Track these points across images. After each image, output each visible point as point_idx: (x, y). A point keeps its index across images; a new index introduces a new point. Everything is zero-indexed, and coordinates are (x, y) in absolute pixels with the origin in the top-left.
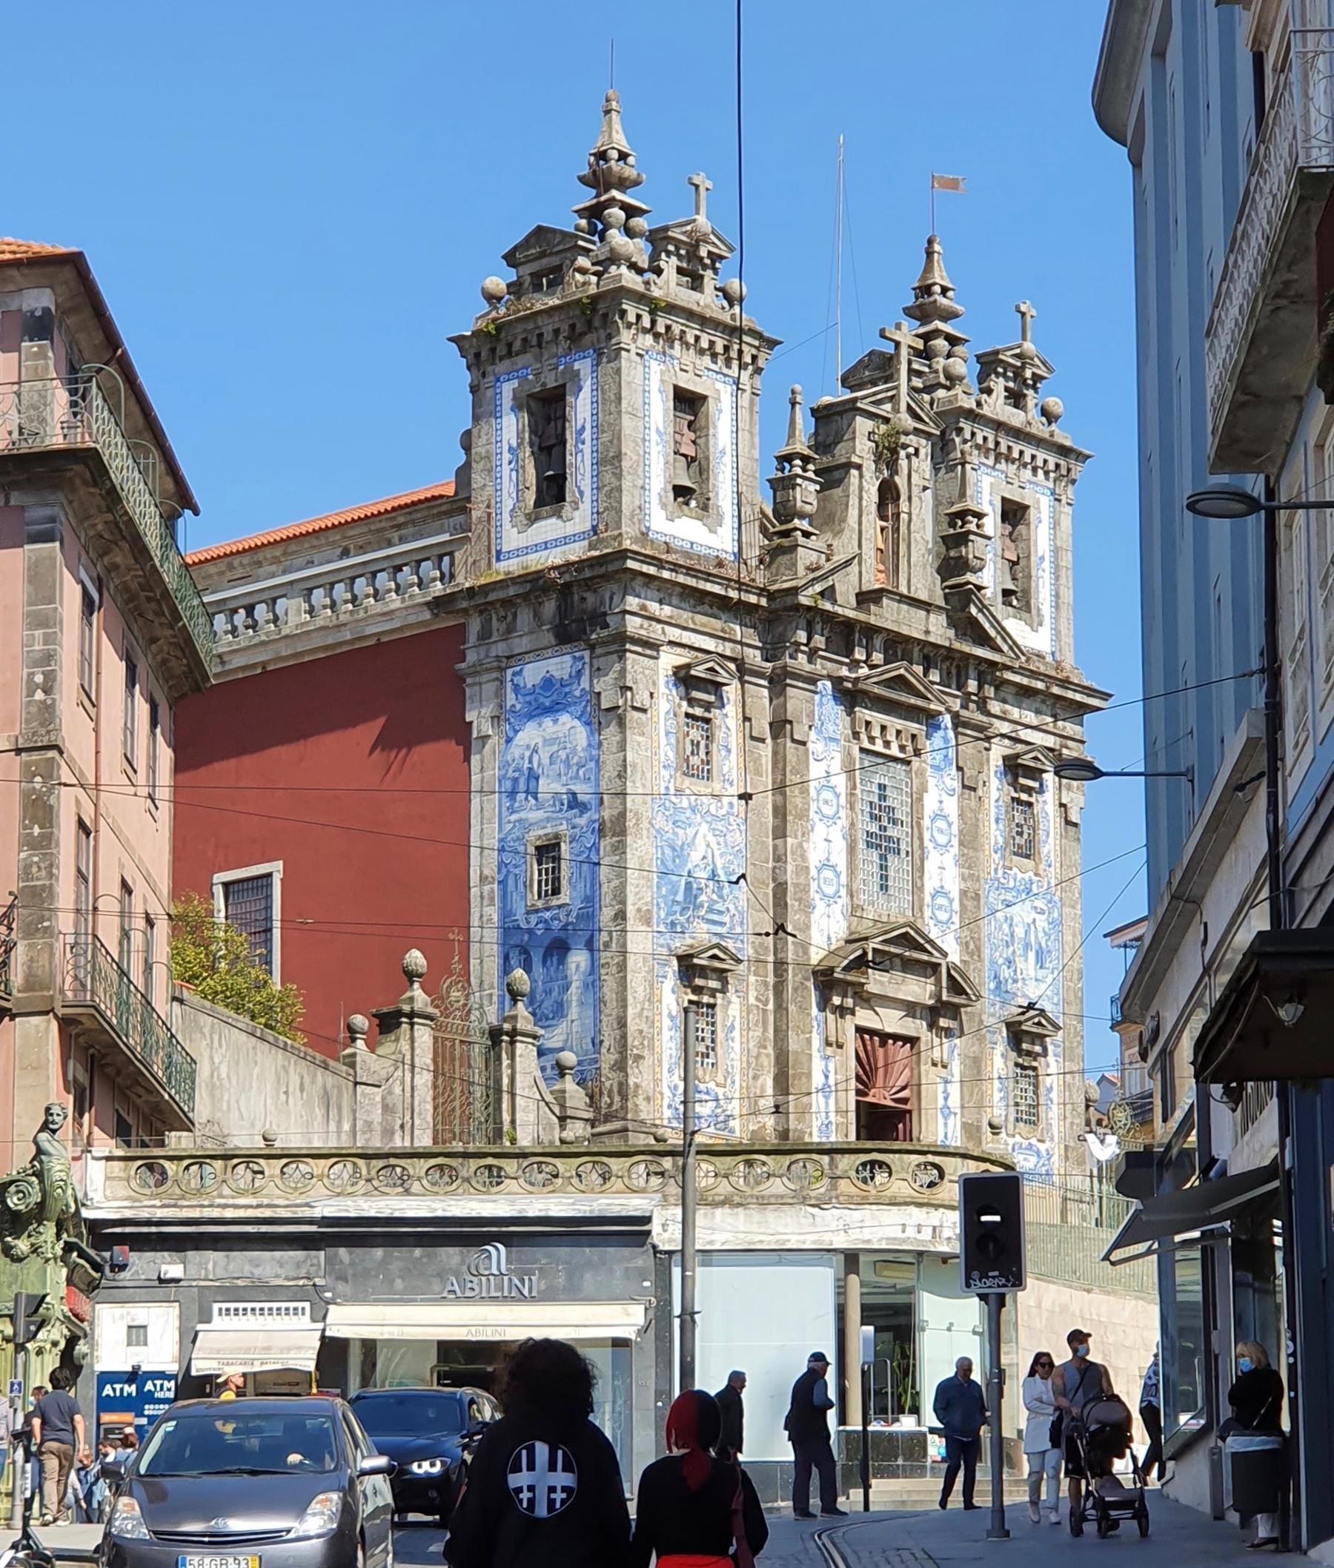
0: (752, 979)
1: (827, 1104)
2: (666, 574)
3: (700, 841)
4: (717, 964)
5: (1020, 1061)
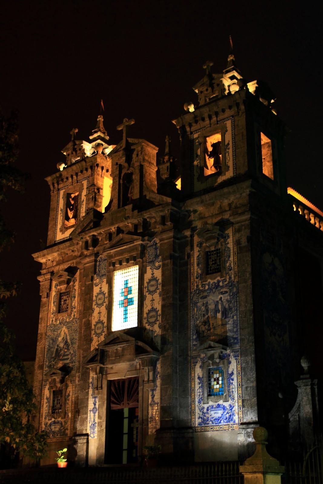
0: (77, 374)
1: (94, 416)
3: (63, 333)
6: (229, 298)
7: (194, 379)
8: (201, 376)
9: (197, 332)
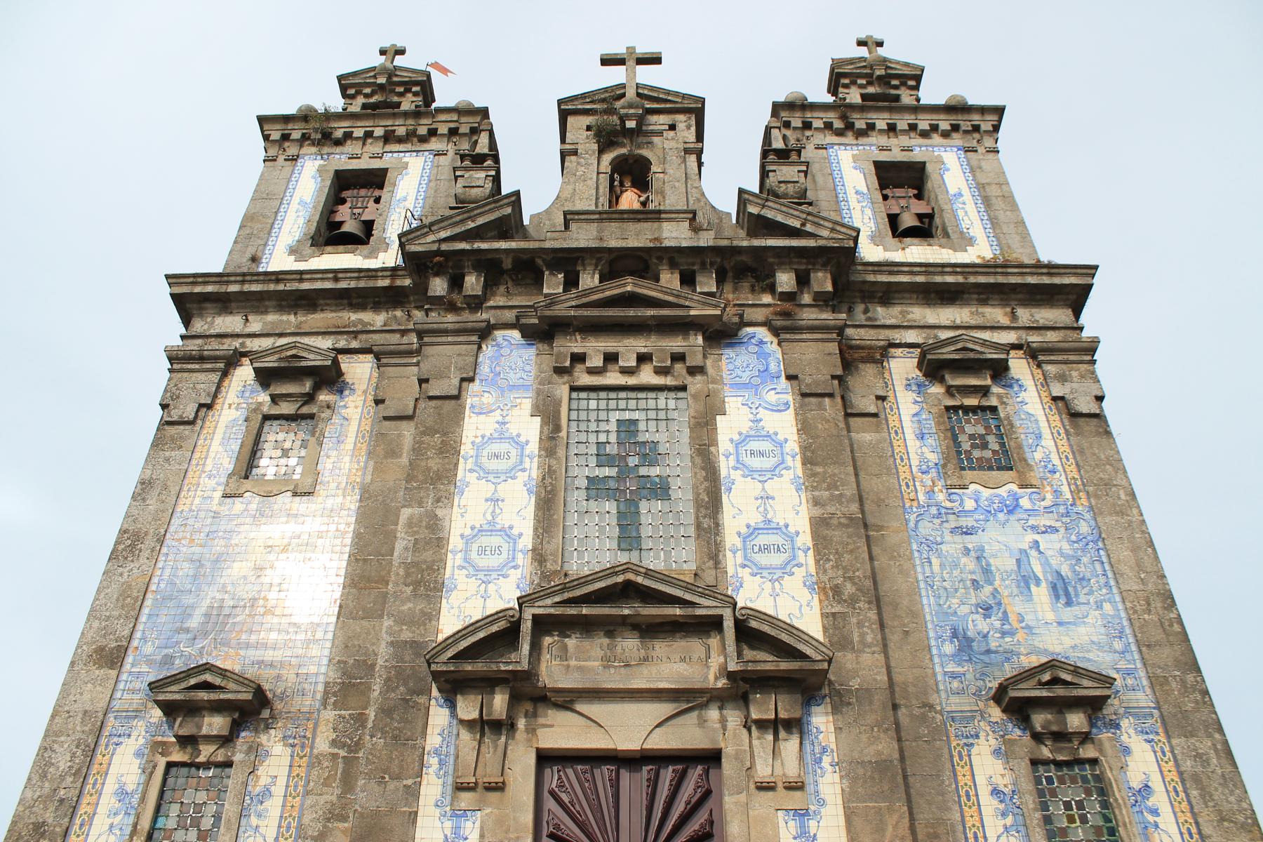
0: (329, 715)
2: (233, 288)
4: (203, 695)
5: (1046, 752)
6: (1066, 546)
7: (972, 795)
8: (1006, 790)
9: (955, 634)
